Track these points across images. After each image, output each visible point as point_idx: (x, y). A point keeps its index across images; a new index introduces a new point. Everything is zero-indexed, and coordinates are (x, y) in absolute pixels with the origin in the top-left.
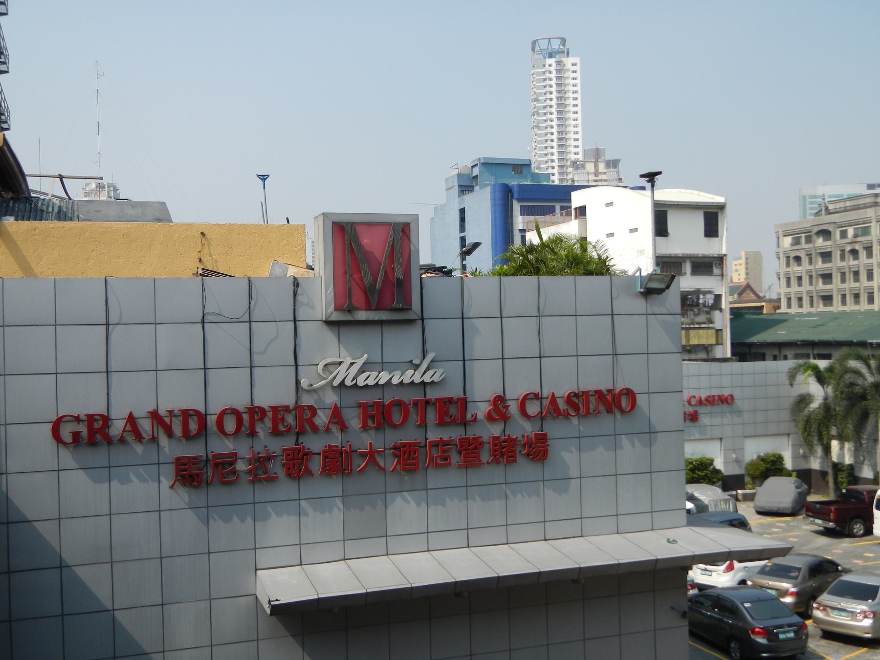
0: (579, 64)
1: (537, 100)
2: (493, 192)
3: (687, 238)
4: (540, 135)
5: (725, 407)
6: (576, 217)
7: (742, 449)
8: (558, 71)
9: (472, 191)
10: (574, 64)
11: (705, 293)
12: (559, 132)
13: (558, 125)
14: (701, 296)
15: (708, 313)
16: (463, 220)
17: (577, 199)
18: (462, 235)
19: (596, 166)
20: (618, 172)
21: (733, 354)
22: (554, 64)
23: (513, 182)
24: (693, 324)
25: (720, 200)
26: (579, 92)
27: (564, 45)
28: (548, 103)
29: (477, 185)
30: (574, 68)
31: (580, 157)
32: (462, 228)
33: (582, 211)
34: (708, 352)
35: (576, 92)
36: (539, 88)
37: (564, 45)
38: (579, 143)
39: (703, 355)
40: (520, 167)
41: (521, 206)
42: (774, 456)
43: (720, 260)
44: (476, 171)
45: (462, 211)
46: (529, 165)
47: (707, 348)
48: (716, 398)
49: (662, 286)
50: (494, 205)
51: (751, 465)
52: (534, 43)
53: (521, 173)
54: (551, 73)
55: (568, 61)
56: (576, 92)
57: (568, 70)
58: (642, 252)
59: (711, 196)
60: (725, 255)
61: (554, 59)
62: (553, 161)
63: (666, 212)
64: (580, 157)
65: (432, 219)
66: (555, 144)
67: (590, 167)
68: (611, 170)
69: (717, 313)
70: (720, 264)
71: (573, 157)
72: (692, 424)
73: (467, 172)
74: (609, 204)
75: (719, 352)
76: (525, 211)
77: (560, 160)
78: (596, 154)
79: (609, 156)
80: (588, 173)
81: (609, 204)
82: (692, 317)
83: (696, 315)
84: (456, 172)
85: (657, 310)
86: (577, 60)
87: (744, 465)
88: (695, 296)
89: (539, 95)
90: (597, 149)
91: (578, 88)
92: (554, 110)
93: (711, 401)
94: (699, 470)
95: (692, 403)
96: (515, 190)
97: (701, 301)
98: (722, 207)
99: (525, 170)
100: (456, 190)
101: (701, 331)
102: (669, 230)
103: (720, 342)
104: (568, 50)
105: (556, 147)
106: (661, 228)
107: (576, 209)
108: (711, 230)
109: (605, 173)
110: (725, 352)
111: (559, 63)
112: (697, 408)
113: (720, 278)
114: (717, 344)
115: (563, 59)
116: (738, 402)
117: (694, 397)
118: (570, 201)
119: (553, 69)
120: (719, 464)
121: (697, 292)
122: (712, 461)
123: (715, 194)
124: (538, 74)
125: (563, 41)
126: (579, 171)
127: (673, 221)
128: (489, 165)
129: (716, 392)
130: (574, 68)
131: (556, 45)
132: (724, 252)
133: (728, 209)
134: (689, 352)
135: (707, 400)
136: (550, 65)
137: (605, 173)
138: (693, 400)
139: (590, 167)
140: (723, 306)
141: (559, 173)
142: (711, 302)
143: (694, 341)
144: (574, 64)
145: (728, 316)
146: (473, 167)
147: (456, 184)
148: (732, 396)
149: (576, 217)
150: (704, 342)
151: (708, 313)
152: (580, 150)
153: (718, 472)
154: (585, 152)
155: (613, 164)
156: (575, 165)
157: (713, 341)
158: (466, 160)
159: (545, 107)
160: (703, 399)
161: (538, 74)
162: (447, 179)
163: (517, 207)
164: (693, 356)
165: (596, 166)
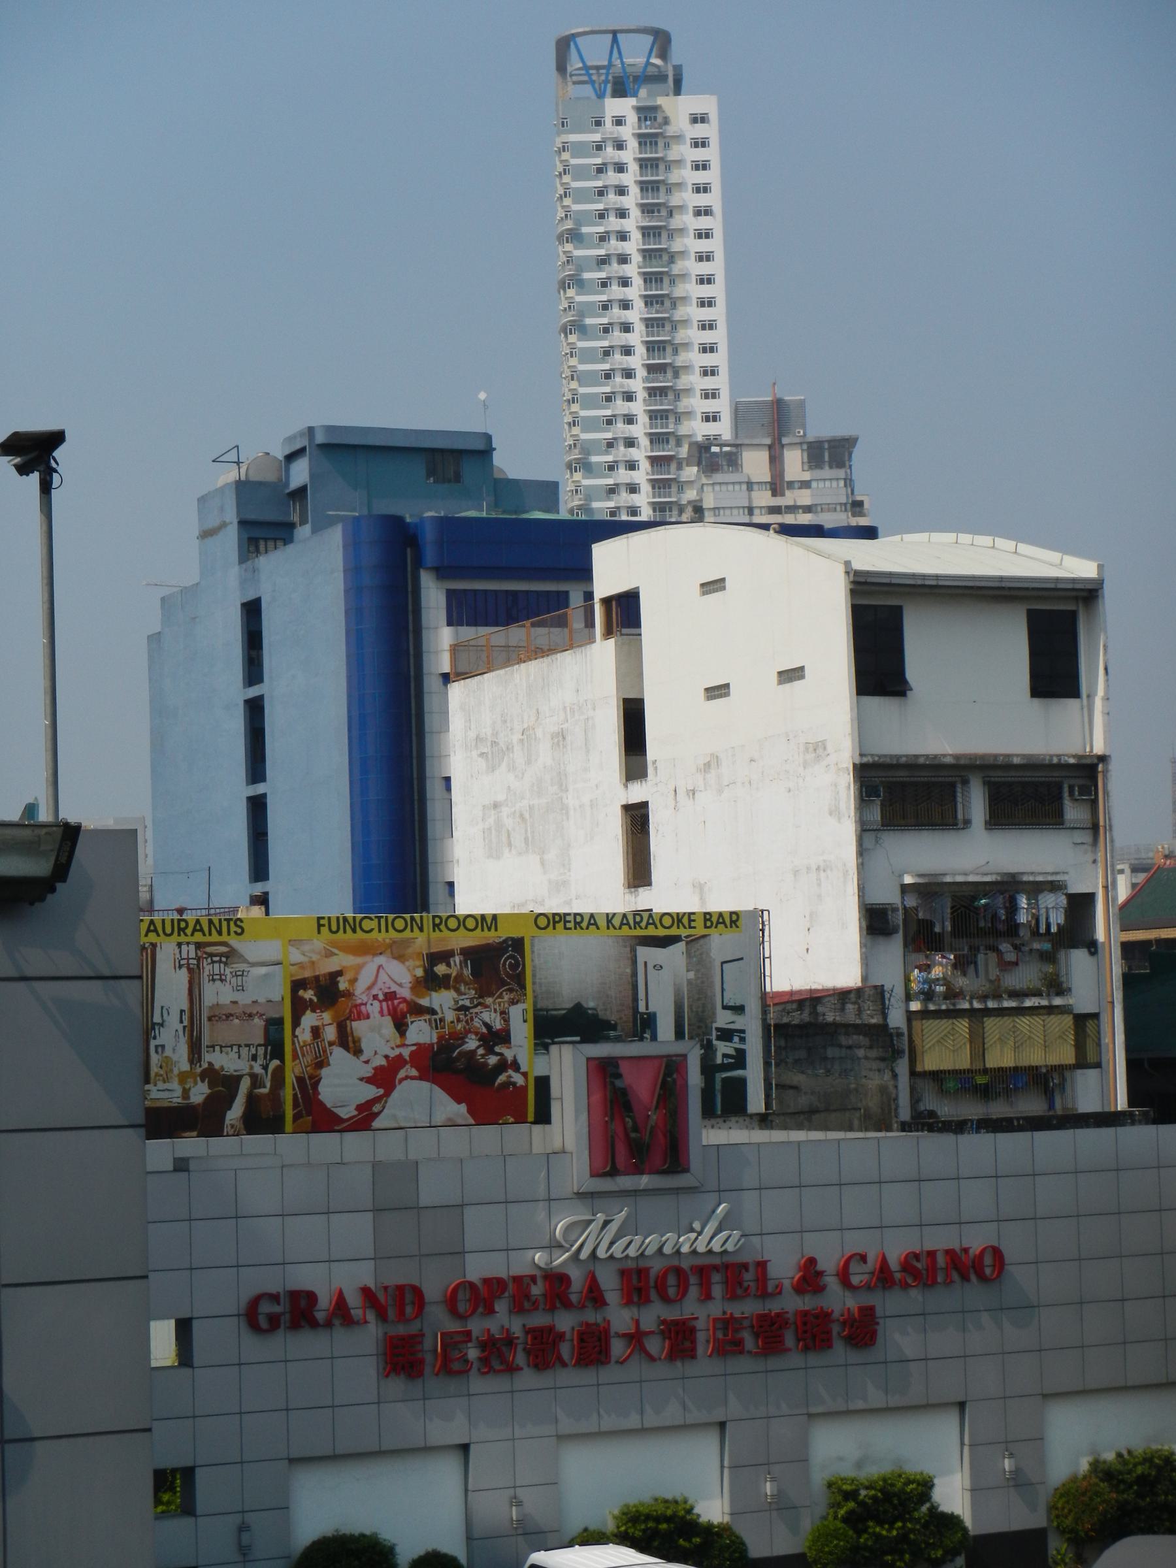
0: (714, 117)
1: (574, 236)
2: (352, 545)
3: (972, 703)
4: (587, 356)
5: (974, 1293)
6: (608, 632)
7: (1038, 1439)
8: (645, 140)
9: (288, 540)
10: (698, 119)
11: (1036, 889)
12: (651, 347)
13: (649, 323)
14: (1023, 902)
15: (1049, 957)
16: (253, 640)
17: (612, 566)
18: (253, 692)
19: (776, 461)
20: (849, 482)
21: (1132, 1100)
22: (632, 118)
23: (426, 508)
24: (997, 997)
25: (1083, 569)
26: (717, 209)
27: (664, 55)
28: (615, 246)
29: (303, 522)
30: (700, 131)
31: (724, 429)
32: (254, 670)
33: (625, 611)
34: (1049, 1095)
35: (707, 212)
36: (581, 196)
37: (664, 55)
38: (721, 382)
39: (1031, 1105)
40: (456, 460)
41: (450, 594)
42: (1148, 1459)
43: (1087, 774)
44: (300, 474)
45: (252, 611)
46: (483, 452)
47: (1045, 1080)
48: (941, 1261)
49: (38, 867)
50: (354, 591)
51: (1072, 1496)
52: (564, 45)
53: (457, 478)
54: (620, 145)
55: (679, 109)
56: (707, 212)
57: (678, 138)
58: (817, 749)
59: (1054, 556)
60: (1103, 759)
61: (632, 101)
62: (630, 443)
63: (896, 615)
64: (724, 429)
65: (155, 639)
66: (637, 385)
67: (756, 464)
68: (827, 472)
69: (1078, 961)
70: (1084, 790)
71: (699, 430)
72: (854, 1356)
73: (270, 476)
74: (713, 586)
75: (1086, 1094)
76: (463, 611)
77: (656, 439)
78: (776, 421)
79: (820, 427)
80: (750, 485)
81: (713, 586)
82: (994, 972)
83: (1007, 966)
84: (230, 475)
85: (36, 960)
86: (707, 104)
87: (1043, 1498)
88: (1000, 900)
89: (582, 218)
90: (779, 406)
91: (713, 199)
92: (632, 270)
93: (921, 1271)
94: (881, 1523)
95: (855, 1280)
96: (429, 536)
97: (1023, 918)
98: (1087, 595)
99: (469, 469)
100: (230, 538)
101: (1024, 1022)
102: (910, 675)
103: (1091, 1057)
104: (678, 70)
105: (641, 395)
106: (879, 666)
107: (606, 601)
108: (1055, 671)
109: (805, 485)
110: (1107, 1090)
111: (647, 113)
112: (874, 1299)
113: (1087, 837)
114: (1082, 1063)
115: (660, 101)
116: (1017, 1273)
117: (863, 1258)
118: (585, 573)
119: (626, 133)
120: (953, 1495)
121: (1009, 887)
122: (926, 1486)
123: (1066, 551)
124: (580, 149)
125: (662, 41)
126: (718, 477)
127: (924, 644)
128: (343, 451)
129: (939, 1240)
130: (700, 131)
131: (636, 54)
132: (1099, 748)
133: (1111, 602)
134: (985, 1093)
135: (907, 1265)
136: (619, 122)
137: (805, 485)
138: (854, 1267)
139: (756, 464)
140: (1100, 935)
141: (654, 483)
142: (1057, 919)
143: (1000, 1057)
144: (698, 119)
145: (1116, 968)
146: (291, 457)
147: (231, 515)
148: (997, 1253)
149: (608, 632)
150: (1035, 1057)
151: (1049, 957)
152: (722, 405)
153: (951, 1522)
154: (740, 413)
155: (832, 453)
156: (708, 457)
157: (1066, 1055)
158: (265, 437)
159: (603, 261)
160: (894, 1264)
161: (580, 149)
162: (202, 500)
163: (433, 596)
164: (998, 1109)
165: (776, 461)
